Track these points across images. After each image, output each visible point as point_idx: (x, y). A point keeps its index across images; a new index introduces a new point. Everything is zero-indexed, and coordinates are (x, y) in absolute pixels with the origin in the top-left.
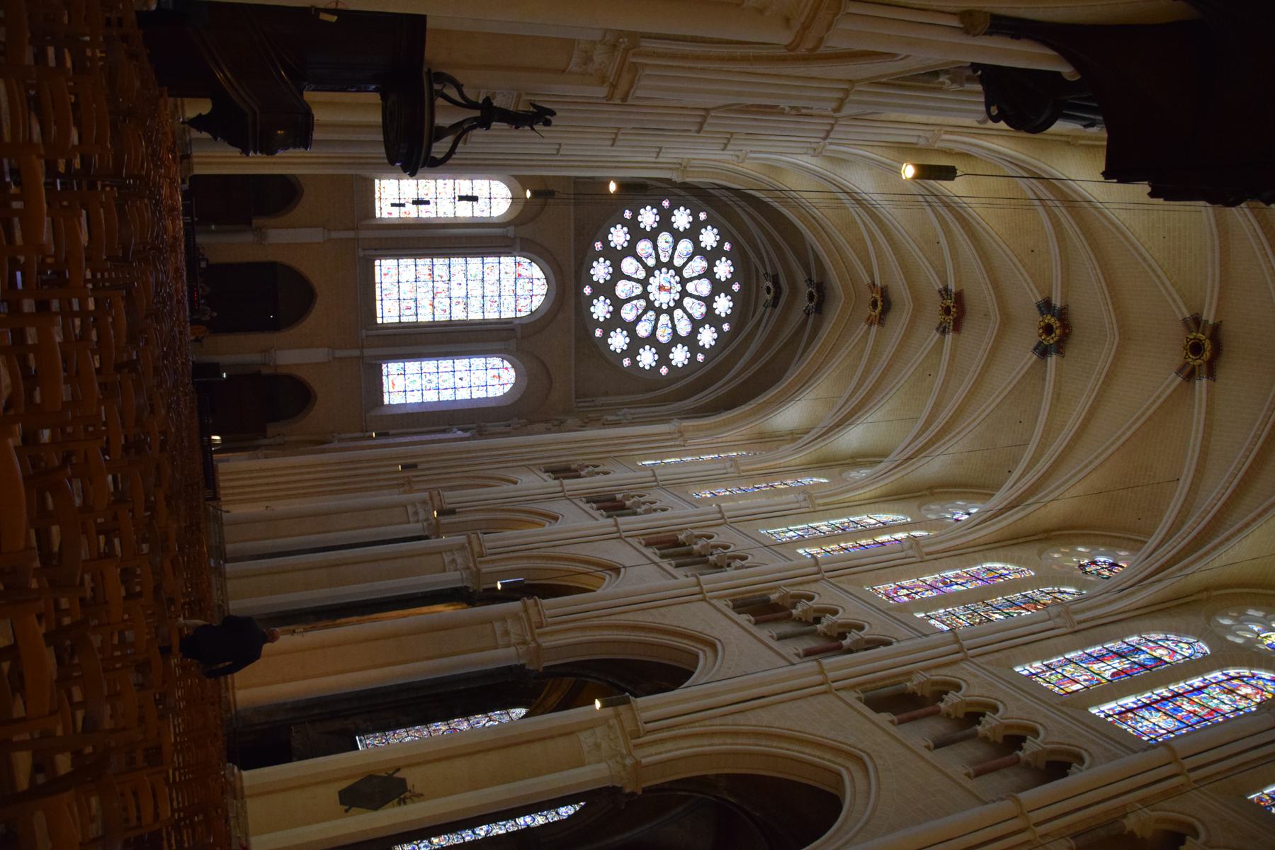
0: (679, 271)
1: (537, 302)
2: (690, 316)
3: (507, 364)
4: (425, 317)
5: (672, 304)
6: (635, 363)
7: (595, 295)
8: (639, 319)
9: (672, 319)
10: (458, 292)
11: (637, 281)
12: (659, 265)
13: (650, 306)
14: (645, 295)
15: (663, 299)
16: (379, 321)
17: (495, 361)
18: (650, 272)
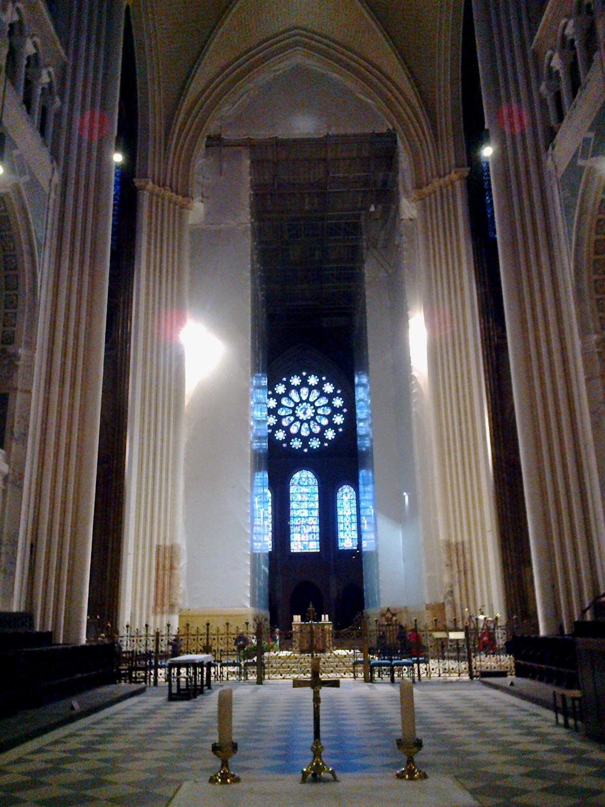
0: (296, 404)
1: (310, 474)
2: (318, 398)
3: (340, 490)
4: (317, 529)
5: (312, 407)
6: (341, 426)
7: (308, 446)
8: (319, 424)
9: (320, 407)
10: (306, 513)
11: (301, 425)
12: (294, 414)
13: (313, 418)
14: (308, 421)
15: (310, 412)
16: (319, 551)
17: (339, 495)
18: (297, 419)
